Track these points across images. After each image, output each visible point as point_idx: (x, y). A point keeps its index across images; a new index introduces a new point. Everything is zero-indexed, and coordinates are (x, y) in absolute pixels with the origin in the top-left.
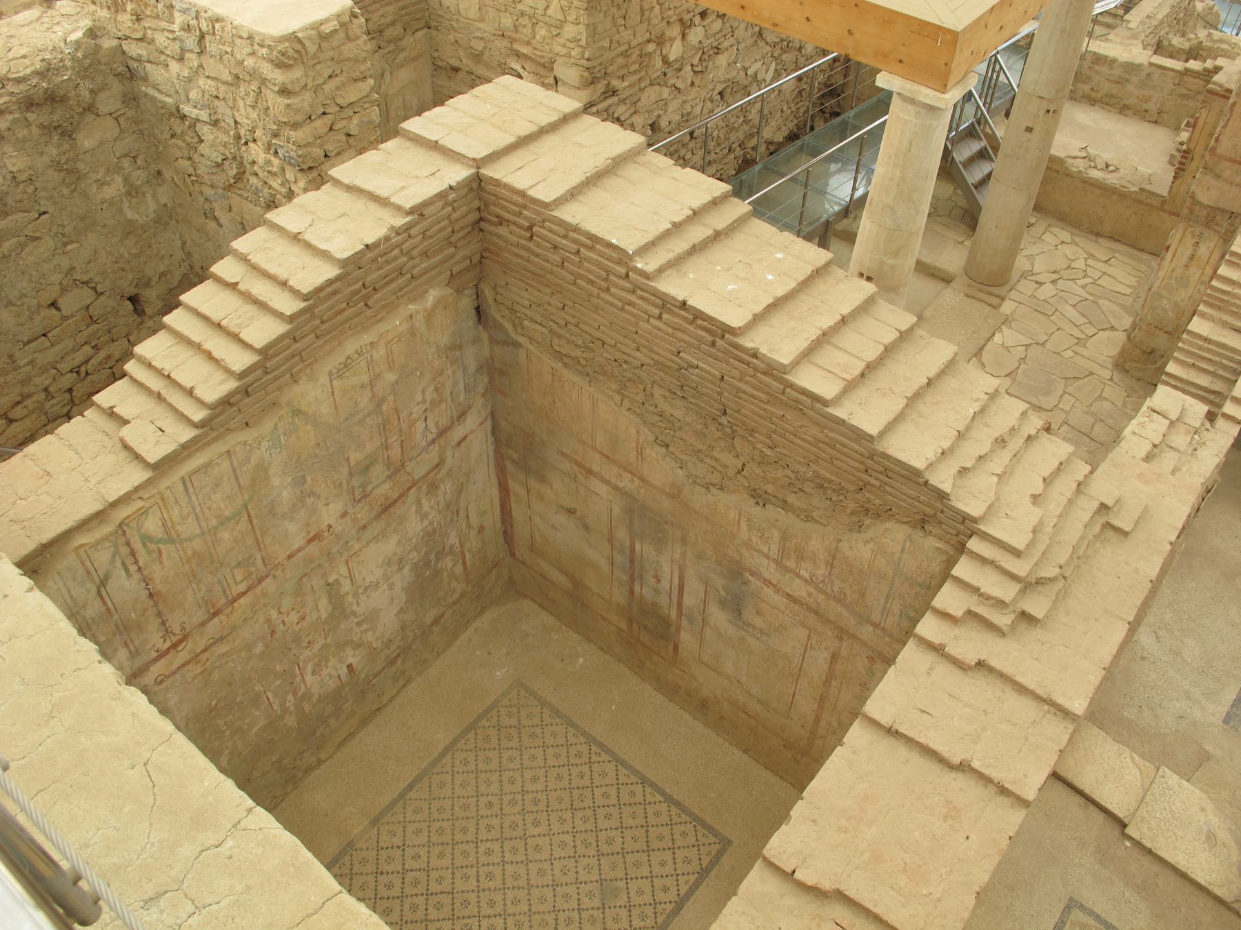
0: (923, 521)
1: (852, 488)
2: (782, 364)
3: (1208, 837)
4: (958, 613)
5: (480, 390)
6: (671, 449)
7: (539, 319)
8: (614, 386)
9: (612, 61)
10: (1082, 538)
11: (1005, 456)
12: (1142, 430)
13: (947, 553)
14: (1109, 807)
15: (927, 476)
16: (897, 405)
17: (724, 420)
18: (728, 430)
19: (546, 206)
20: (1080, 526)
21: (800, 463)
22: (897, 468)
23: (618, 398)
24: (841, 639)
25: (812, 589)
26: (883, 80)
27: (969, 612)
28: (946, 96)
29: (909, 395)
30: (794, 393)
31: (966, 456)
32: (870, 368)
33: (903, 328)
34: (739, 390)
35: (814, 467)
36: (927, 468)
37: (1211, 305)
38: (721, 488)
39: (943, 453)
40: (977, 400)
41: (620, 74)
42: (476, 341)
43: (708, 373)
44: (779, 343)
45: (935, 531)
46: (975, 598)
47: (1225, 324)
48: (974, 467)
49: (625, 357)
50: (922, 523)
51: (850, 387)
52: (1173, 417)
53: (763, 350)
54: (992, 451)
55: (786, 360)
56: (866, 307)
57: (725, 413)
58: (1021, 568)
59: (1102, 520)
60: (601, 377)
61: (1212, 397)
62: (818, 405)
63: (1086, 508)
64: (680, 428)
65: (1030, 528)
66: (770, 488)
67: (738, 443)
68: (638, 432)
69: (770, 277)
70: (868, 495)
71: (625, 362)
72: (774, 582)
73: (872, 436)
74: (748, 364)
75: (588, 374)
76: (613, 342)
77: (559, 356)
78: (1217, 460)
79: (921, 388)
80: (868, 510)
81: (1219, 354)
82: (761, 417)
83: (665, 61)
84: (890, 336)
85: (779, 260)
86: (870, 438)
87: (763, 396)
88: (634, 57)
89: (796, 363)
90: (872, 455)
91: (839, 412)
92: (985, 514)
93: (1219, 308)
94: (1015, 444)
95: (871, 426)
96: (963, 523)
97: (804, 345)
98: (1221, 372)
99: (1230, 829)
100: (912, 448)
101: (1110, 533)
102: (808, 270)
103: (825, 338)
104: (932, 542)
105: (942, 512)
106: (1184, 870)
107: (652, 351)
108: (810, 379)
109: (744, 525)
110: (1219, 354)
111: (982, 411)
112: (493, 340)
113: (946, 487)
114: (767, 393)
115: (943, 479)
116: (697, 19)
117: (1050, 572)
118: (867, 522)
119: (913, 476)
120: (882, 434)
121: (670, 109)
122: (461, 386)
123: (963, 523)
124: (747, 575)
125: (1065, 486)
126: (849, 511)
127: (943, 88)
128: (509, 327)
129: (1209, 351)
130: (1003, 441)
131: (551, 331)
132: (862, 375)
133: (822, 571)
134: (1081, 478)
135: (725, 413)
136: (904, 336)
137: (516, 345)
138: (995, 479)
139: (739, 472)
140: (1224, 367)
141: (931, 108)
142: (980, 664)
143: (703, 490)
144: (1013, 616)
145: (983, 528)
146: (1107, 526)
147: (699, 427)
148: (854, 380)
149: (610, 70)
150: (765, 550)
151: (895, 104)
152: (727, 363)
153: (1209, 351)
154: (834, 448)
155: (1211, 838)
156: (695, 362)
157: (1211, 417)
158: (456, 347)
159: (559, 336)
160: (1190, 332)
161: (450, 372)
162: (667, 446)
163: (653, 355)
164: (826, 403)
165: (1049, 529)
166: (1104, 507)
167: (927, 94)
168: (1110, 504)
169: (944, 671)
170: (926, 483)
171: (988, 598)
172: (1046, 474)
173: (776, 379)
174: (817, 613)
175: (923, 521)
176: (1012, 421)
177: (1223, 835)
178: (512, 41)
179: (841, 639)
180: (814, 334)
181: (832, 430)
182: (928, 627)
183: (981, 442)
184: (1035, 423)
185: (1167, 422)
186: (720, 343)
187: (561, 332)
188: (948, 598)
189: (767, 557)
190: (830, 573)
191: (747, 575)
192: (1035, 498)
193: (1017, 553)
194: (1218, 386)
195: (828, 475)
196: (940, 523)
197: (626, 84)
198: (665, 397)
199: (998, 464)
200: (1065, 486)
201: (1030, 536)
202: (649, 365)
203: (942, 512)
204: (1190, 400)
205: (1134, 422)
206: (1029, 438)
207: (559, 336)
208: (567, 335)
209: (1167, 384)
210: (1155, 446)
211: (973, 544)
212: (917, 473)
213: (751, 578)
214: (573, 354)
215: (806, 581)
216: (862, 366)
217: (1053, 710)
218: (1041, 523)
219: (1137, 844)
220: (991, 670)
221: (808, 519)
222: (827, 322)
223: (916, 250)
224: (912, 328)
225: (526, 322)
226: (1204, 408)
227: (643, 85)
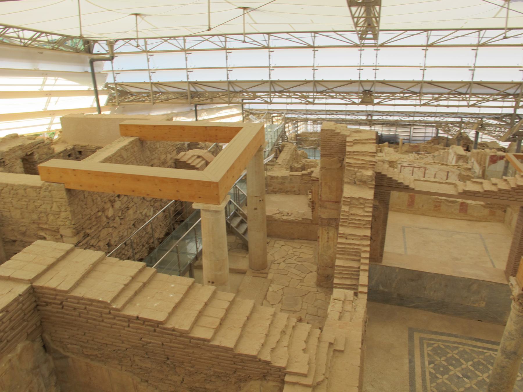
0: (264, 376)
1: (231, 373)
2: (186, 331)
5: (53, 384)
6: (149, 382)
7: (74, 342)
8: (116, 362)
9: (84, 223)
10: (328, 359)
11: (287, 337)
12: (334, 309)
13: (278, 386)
15: (259, 357)
16: (238, 332)
17: (169, 362)
18: (172, 366)
19: (67, 292)
21: (207, 370)
22: (246, 358)
23: (119, 367)
26: (195, 206)
28: (221, 206)
29: (242, 326)
30: (195, 341)
31: (272, 343)
32: (223, 320)
33: (231, 300)
34: (171, 347)
35: (213, 369)
36: (258, 354)
37: (340, 254)
39: (262, 345)
40: (269, 319)
41: (89, 227)
42: (46, 361)
44: (182, 322)
45: (271, 378)
47: (347, 259)
48: (276, 347)
49: (118, 348)
50: (264, 377)
51: (217, 331)
52: (343, 299)
53: (177, 327)
54: (281, 337)
55: (187, 328)
56: (214, 295)
57: (168, 359)
58: (309, 381)
59: (332, 349)
60: (109, 360)
61: (353, 287)
62: (206, 343)
63: (325, 347)
65: (306, 363)
66: (197, 385)
67: (178, 369)
68: (133, 379)
69: (171, 296)
70: (239, 373)
71: (119, 350)
73: (232, 349)
74: (172, 335)
75: (103, 361)
76: (110, 343)
77: (88, 356)
78: (364, 310)
79: (245, 321)
80: (240, 380)
81: (350, 271)
82: (184, 355)
83: (107, 217)
84: (226, 305)
85: (173, 288)
86: (231, 349)
87: (182, 346)
88: (94, 219)
89: (192, 328)
91: (216, 343)
92: (287, 364)
93: (343, 254)
94: (289, 331)
96: (280, 371)
97: (193, 319)
98: (353, 277)
100: (249, 348)
101: (337, 353)
102: (186, 288)
103: (201, 314)
104: (271, 384)
105: (270, 370)
107: (129, 342)
108: (201, 333)
110: (350, 271)
111: (272, 323)
112: (55, 359)
113: (268, 359)
114: (183, 345)
115: (266, 356)
116: (117, 199)
117: (320, 378)
118: (242, 384)
119: (254, 359)
120: (236, 346)
121: (114, 236)
123: (280, 371)
125: (314, 341)
126: (233, 383)
127: (219, 203)
128: (61, 350)
129: (346, 270)
130: (284, 332)
131: (81, 346)
132: (220, 324)
134: (318, 336)
135: (168, 359)
136: (232, 303)
137: (66, 357)
138: (286, 348)
139: (182, 382)
140: (353, 275)
141: (216, 212)
145: (288, 370)
146: (336, 351)
147: (159, 368)
148: (217, 327)
149: (84, 227)
151: (203, 213)
152: (163, 337)
153: (346, 270)
154: (218, 358)
156: (149, 341)
157: (356, 294)
158: (36, 367)
159: (86, 347)
160: (337, 266)
162: (147, 381)
163: (130, 343)
164: (209, 341)
166: (331, 344)
167: (213, 207)
168: (332, 342)
170: (260, 360)
172: (305, 339)
173: (185, 337)
175: (264, 376)
176: (285, 322)
178: (39, 224)
180: (195, 314)
181: (215, 351)
183: (275, 336)
184: (294, 320)
185: (341, 302)
186: (158, 329)
187: (86, 345)
192: (304, 350)
193: (305, 376)
194: (354, 282)
195: (219, 371)
196: (271, 374)
197: (93, 230)
198: (140, 360)
199: (285, 343)
200: (314, 341)
201: (308, 366)
202: (129, 348)
203: (270, 370)
204: (346, 291)
205: (330, 306)
206: (294, 327)
207: (86, 347)
208: (89, 346)
209: (336, 287)
210: (341, 313)
211: (287, 378)
212: (254, 357)
214: (94, 354)
216: (219, 321)
218: (310, 359)
222: (199, 307)
223: (228, 265)
224: (234, 299)
225: (69, 346)
226: (352, 292)
227: (100, 229)
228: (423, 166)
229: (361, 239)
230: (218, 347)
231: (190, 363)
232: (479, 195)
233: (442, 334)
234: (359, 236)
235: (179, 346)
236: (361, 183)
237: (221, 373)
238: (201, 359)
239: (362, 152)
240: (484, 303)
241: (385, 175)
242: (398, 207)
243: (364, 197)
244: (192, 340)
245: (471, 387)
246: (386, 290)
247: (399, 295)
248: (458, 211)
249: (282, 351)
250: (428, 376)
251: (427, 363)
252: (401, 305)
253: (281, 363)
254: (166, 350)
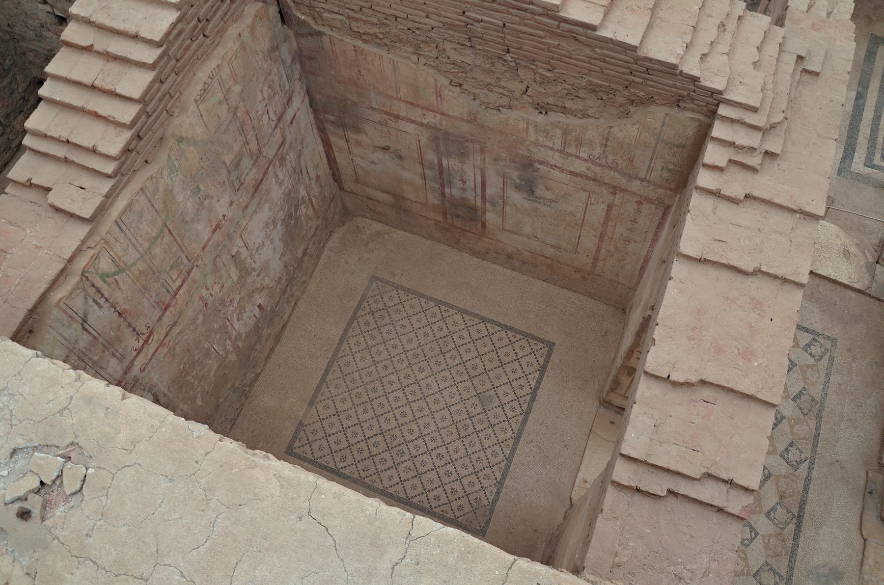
3: (844, 253)
4: (722, 163)
5: (297, 76)
6: (464, 87)
7: (336, 9)
8: (410, 49)
11: (728, 36)
13: (699, 120)
17: (508, 57)
20: (788, 77)
21: (575, 77)
22: (656, 66)
23: (414, 58)
24: (614, 194)
25: (589, 165)
27: (730, 161)
35: (587, 78)
38: (510, 108)
42: (286, 38)
43: (492, 23)
45: (689, 105)
46: (731, 149)
49: (417, 25)
50: (678, 102)
57: (508, 51)
59: (800, 69)
60: (397, 45)
62: (589, 31)
64: (471, 70)
66: (550, 100)
67: (521, 72)
68: (435, 80)
70: (632, 90)
71: (418, 29)
72: (559, 165)
74: (526, 10)
75: (386, 45)
76: (405, 15)
77: (359, 35)
80: (633, 101)
82: (541, 49)
86: (634, 48)
90: (638, 60)
94: (731, 25)
95: (633, 40)
100: (663, 48)
101: (807, 76)
105: (694, 91)
106: (834, 278)
107: (440, 15)
109: (531, 130)
112: (297, 35)
113: (695, 73)
114: (544, 30)
115: (691, 67)
117: (778, 117)
118: (632, 109)
119: (670, 69)
122: (285, 78)
123: (711, 96)
124: (536, 165)
125: (771, 49)
128: (311, 21)
131: (348, 17)
133: (598, 151)
134: (780, 40)
135: (508, 51)
137: (320, 34)
139: (524, 93)
143: (494, 112)
144: (761, 156)
145: (727, 97)
147: (487, 66)
150: (550, 144)
154: (604, 61)
155: (846, 253)
156: (480, 17)
158: (275, 48)
159: (356, 20)
161: (275, 70)
162: (461, 85)
163: (442, 19)
164: (594, 28)
165: (770, 86)
166: (800, 58)
168: (803, 54)
169: (725, 209)
170: (681, 72)
172: (758, 44)
174: (595, 180)
177: (853, 250)
179: (614, 194)
181: (601, 48)
182: (704, 179)
187: (357, 16)
188: (712, 154)
189: (552, 149)
190: (604, 151)
191: (536, 165)
193: (755, 110)
196: (693, 99)
198: (455, 49)
199: (723, 48)
202: (439, 27)
207: (356, 20)
208: (363, 17)
211: (723, 110)
213: (539, 166)
214: (371, 32)
215: (585, 160)
217: (802, 216)
220: (755, 198)
221: (585, 115)
225: (325, 15)
230: (611, 41)
231: (549, 63)
235: (535, 31)
237: (601, 86)
238: (570, 58)
244: (562, 24)
249: (717, 61)
253: (717, 84)
254: (508, 37)
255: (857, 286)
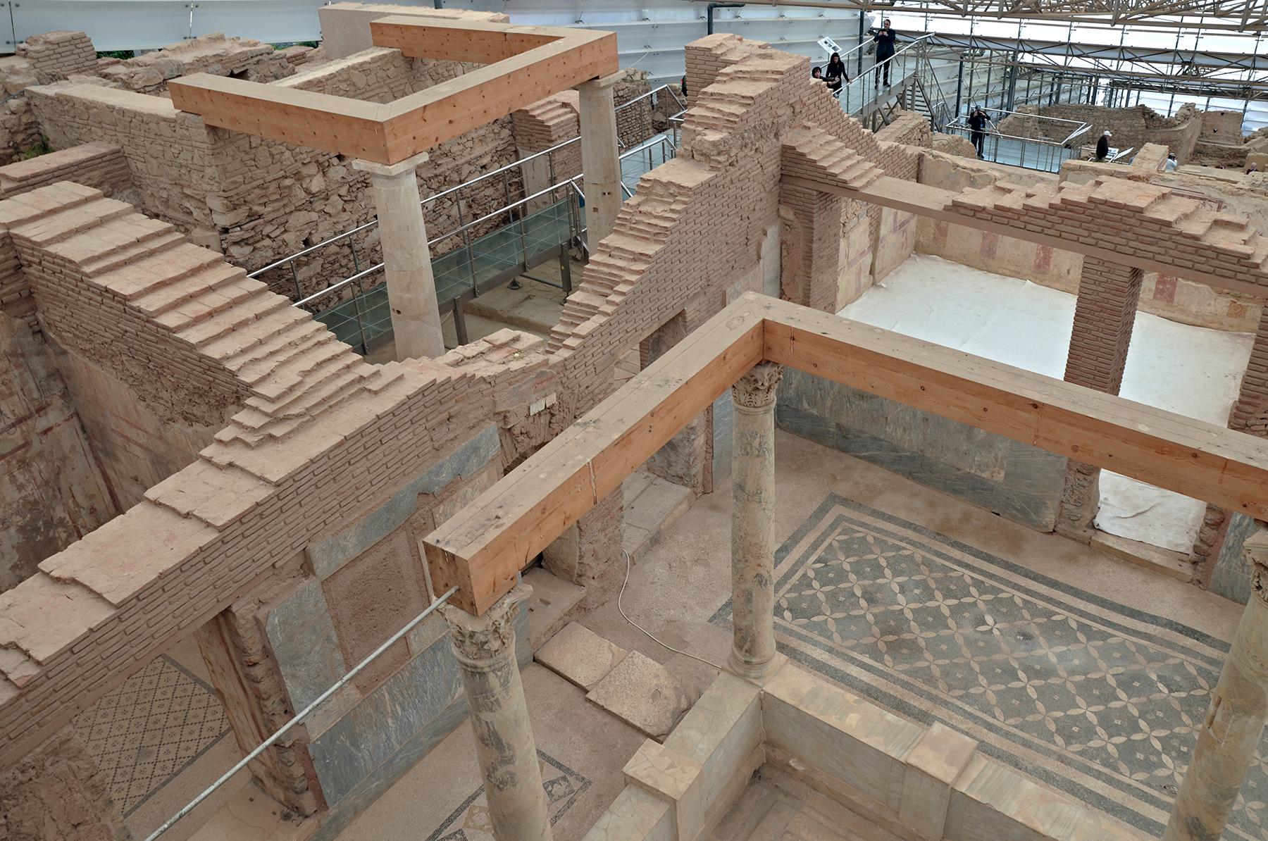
9: (249, 192)
14: (577, 680)
19: (40, 244)
41: (262, 201)
83: (307, 191)
88: (272, 189)
99: (675, 688)
116: (335, 161)
121: (321, 228)
142: (231, 465)
149: (248, 198)
171: (247, 428)
178: (182, 187)
197: (269, 209)
219: (595, 704)
227: (288, 210)
228: (1215, 195)
229: (634, 260)
232: (983, 215)
233: (890, 519)
234: (633, 253)
236: (703, 158)
239: (727, 96)
240: (1003, 473)
241: (803, 155)
242: (1013, 268)
243: (677, 182)
245: (864, 616)
246: (815, 412)
247: (839, 426)
248: (1151, 296)
250: (795, 579)
251: (814, 558)
252: (845, 450)
255: (648, 730)
